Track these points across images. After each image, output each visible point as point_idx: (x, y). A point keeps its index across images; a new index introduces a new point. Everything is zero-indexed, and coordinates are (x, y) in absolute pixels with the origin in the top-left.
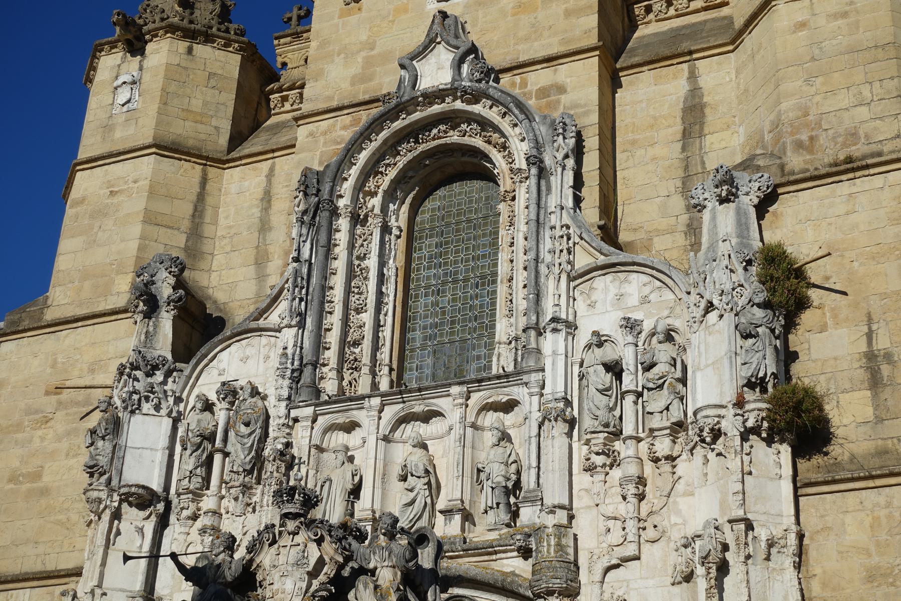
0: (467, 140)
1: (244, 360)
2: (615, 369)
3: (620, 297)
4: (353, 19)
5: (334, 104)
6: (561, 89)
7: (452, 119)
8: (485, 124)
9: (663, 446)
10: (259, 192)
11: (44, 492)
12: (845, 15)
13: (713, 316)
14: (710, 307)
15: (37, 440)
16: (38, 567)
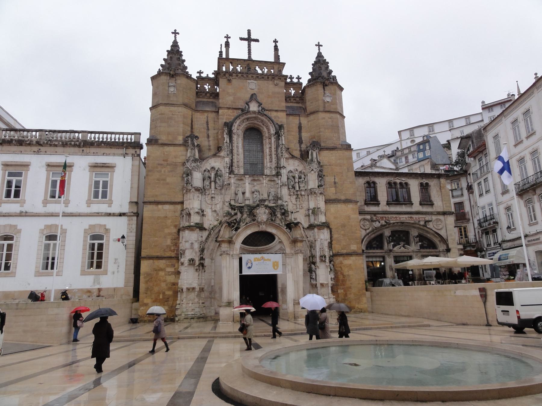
0: (258, 123)
1: (215, 162)
2: (294, 177)
3: (294, 164)
4: (230, 87)
5: (228, 106)
6: (279, 118)
7: (256, 118)
8: (262, 121)
9: (303, 193)
10: (206, 120)
11: (168, 184)
12: (331, 118)
13: (312, 172)
14: (313, 170)
15: (163, 172)
16: (169, 200)
